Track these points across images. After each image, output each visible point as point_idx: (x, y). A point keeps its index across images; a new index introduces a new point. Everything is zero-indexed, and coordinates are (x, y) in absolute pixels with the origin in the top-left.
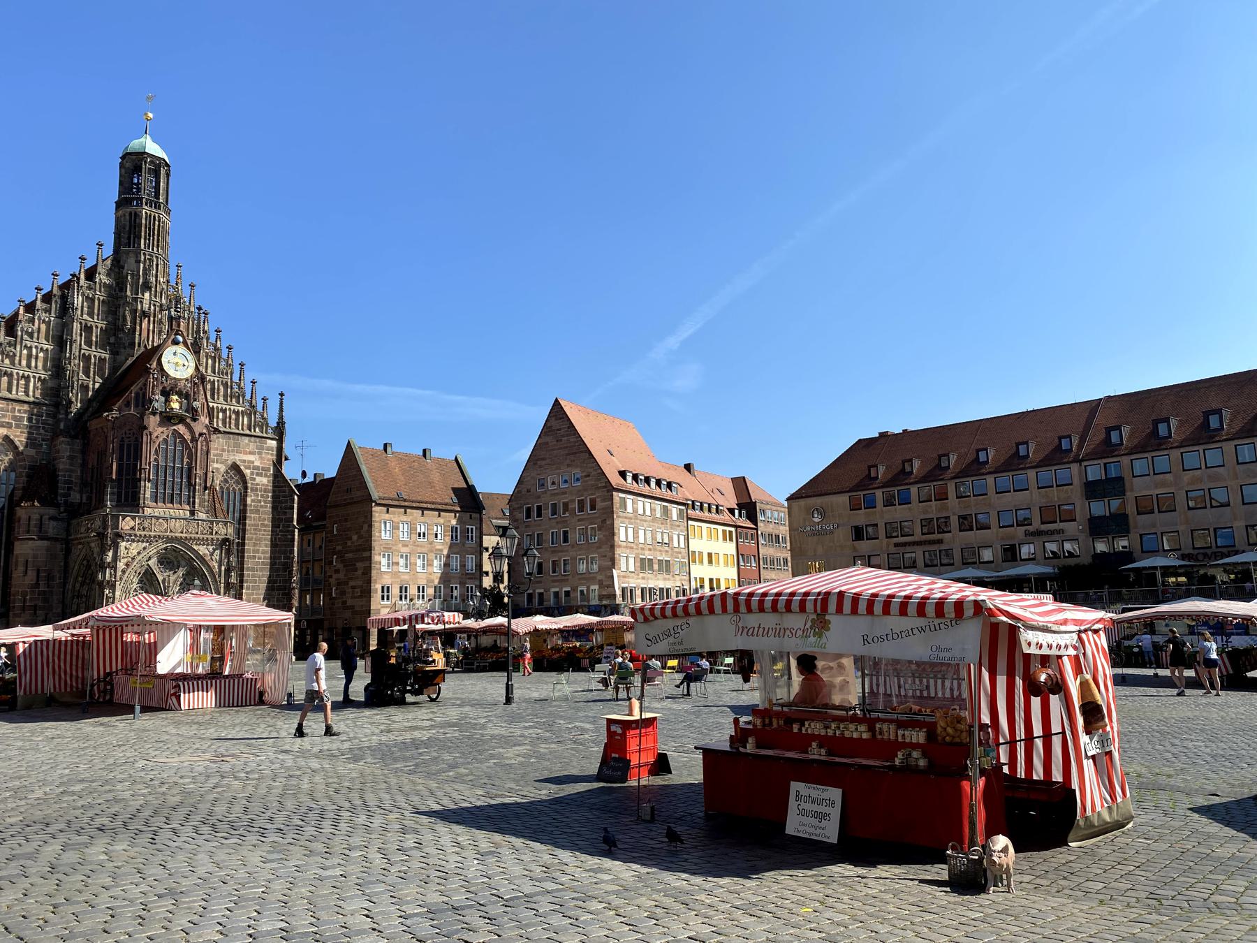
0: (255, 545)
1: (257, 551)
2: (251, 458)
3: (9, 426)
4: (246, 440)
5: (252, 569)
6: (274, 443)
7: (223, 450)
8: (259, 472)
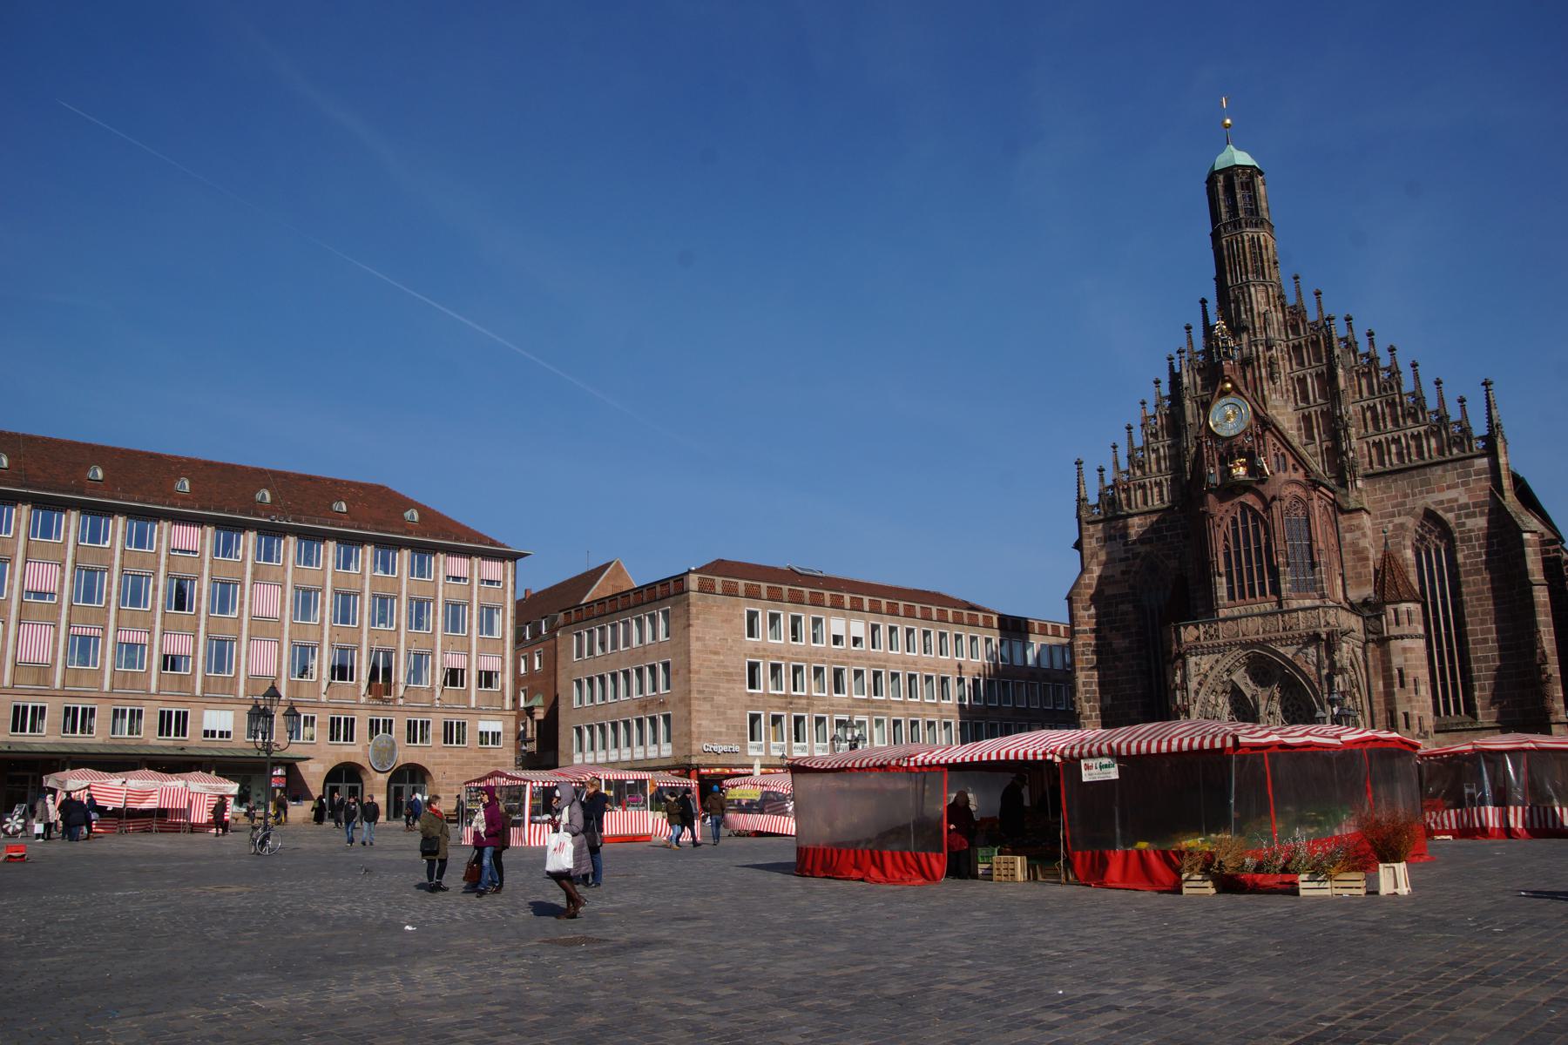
4: (1439, 471)
6: (1483, 462)
7: (1406, 496)
8: (1466, 511)
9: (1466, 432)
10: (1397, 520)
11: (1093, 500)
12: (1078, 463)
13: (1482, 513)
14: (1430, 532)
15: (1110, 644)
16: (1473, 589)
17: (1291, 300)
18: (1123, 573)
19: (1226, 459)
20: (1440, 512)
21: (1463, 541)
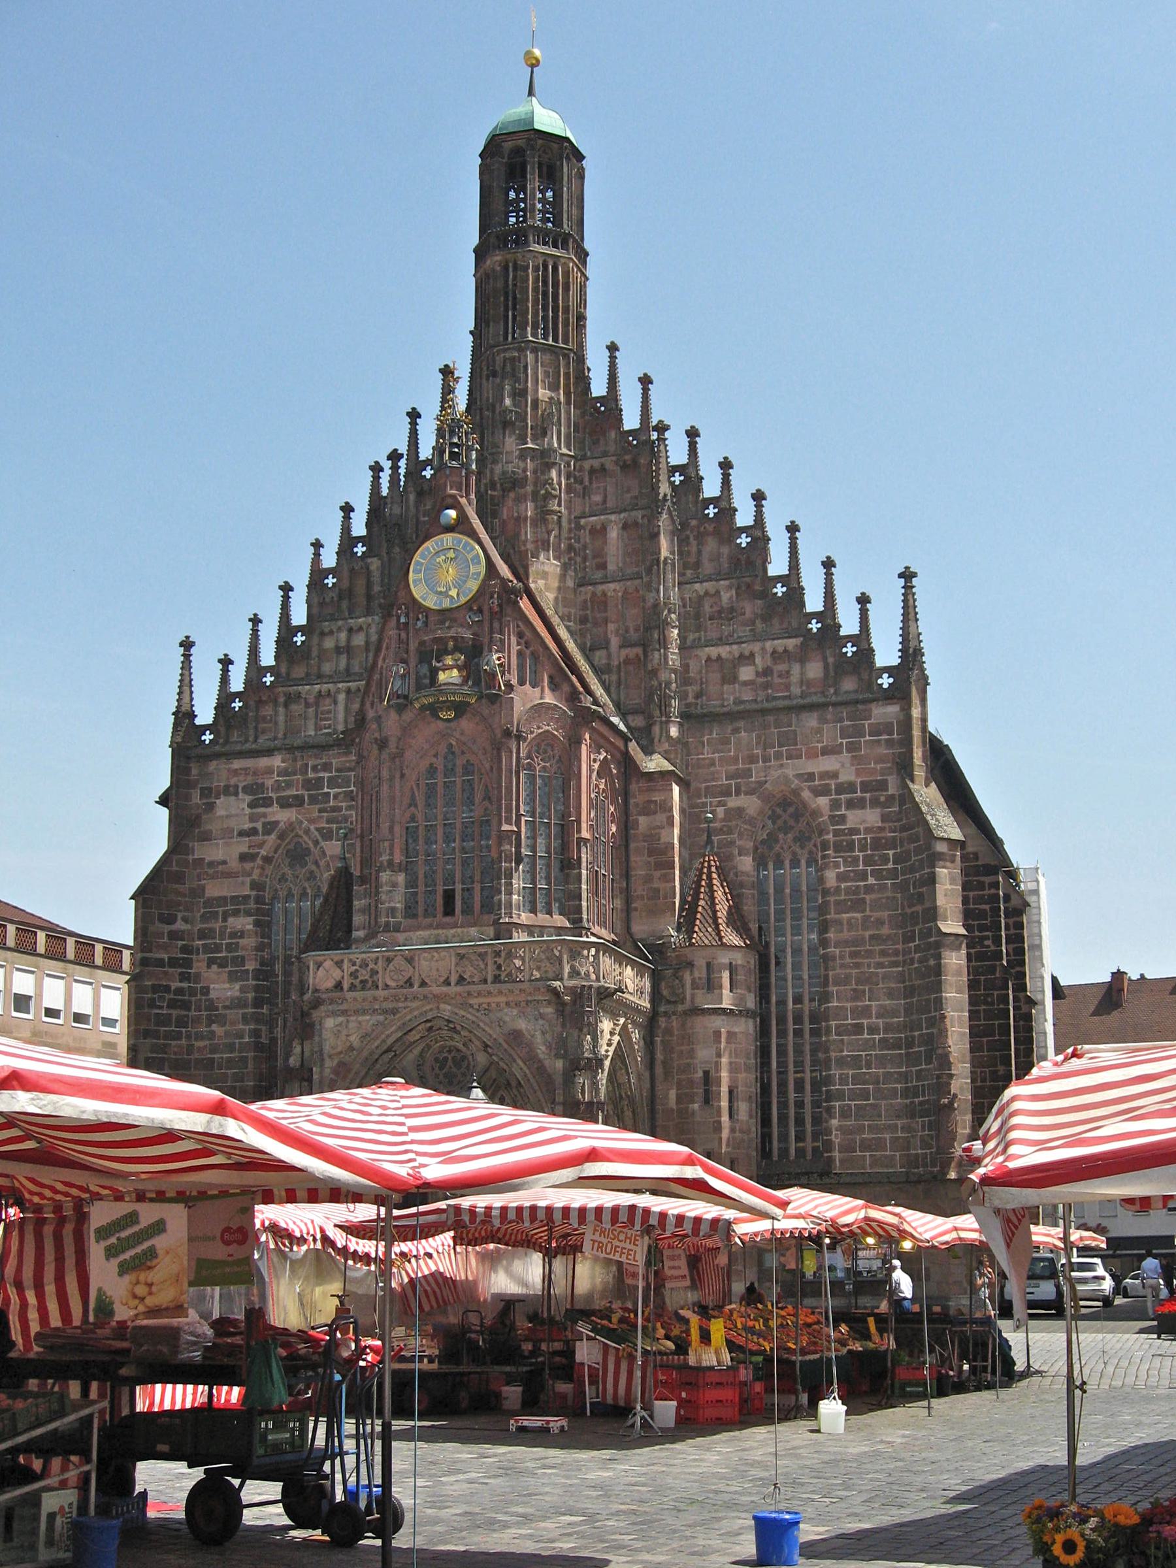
0: (857, 995)
1: (866, 1012)
2: (828, 764)
3: (298, 802)
4: (811, 721)
5: (856, 1061)
7: (752, 759)
8: (850, 795)
9: (866, 653)
10: (733, 802)
11: (205, 714)
12: (187, 644)
13: (875, 803)
14: (786, 829)
15: (206, 991)
16: (846, 935)
17: (598, 388)
18: (243, 858)
19: (431, 656)
20: (806, 794)
21: (838, 848)
